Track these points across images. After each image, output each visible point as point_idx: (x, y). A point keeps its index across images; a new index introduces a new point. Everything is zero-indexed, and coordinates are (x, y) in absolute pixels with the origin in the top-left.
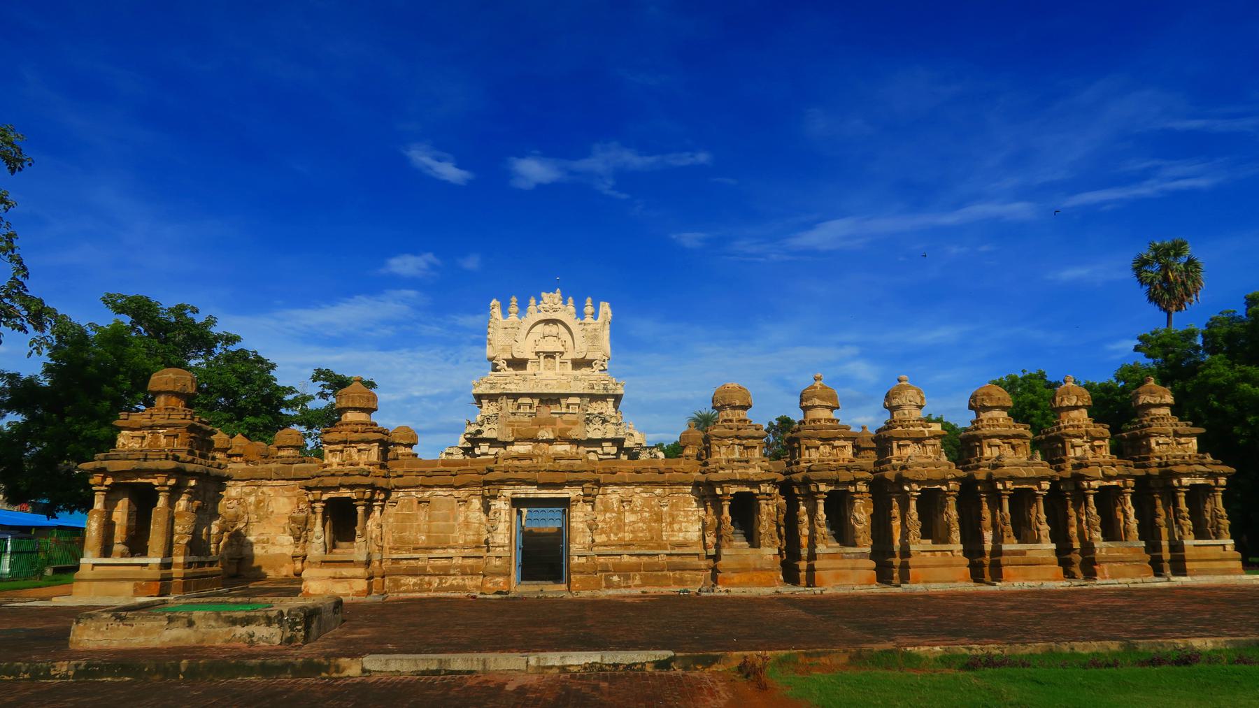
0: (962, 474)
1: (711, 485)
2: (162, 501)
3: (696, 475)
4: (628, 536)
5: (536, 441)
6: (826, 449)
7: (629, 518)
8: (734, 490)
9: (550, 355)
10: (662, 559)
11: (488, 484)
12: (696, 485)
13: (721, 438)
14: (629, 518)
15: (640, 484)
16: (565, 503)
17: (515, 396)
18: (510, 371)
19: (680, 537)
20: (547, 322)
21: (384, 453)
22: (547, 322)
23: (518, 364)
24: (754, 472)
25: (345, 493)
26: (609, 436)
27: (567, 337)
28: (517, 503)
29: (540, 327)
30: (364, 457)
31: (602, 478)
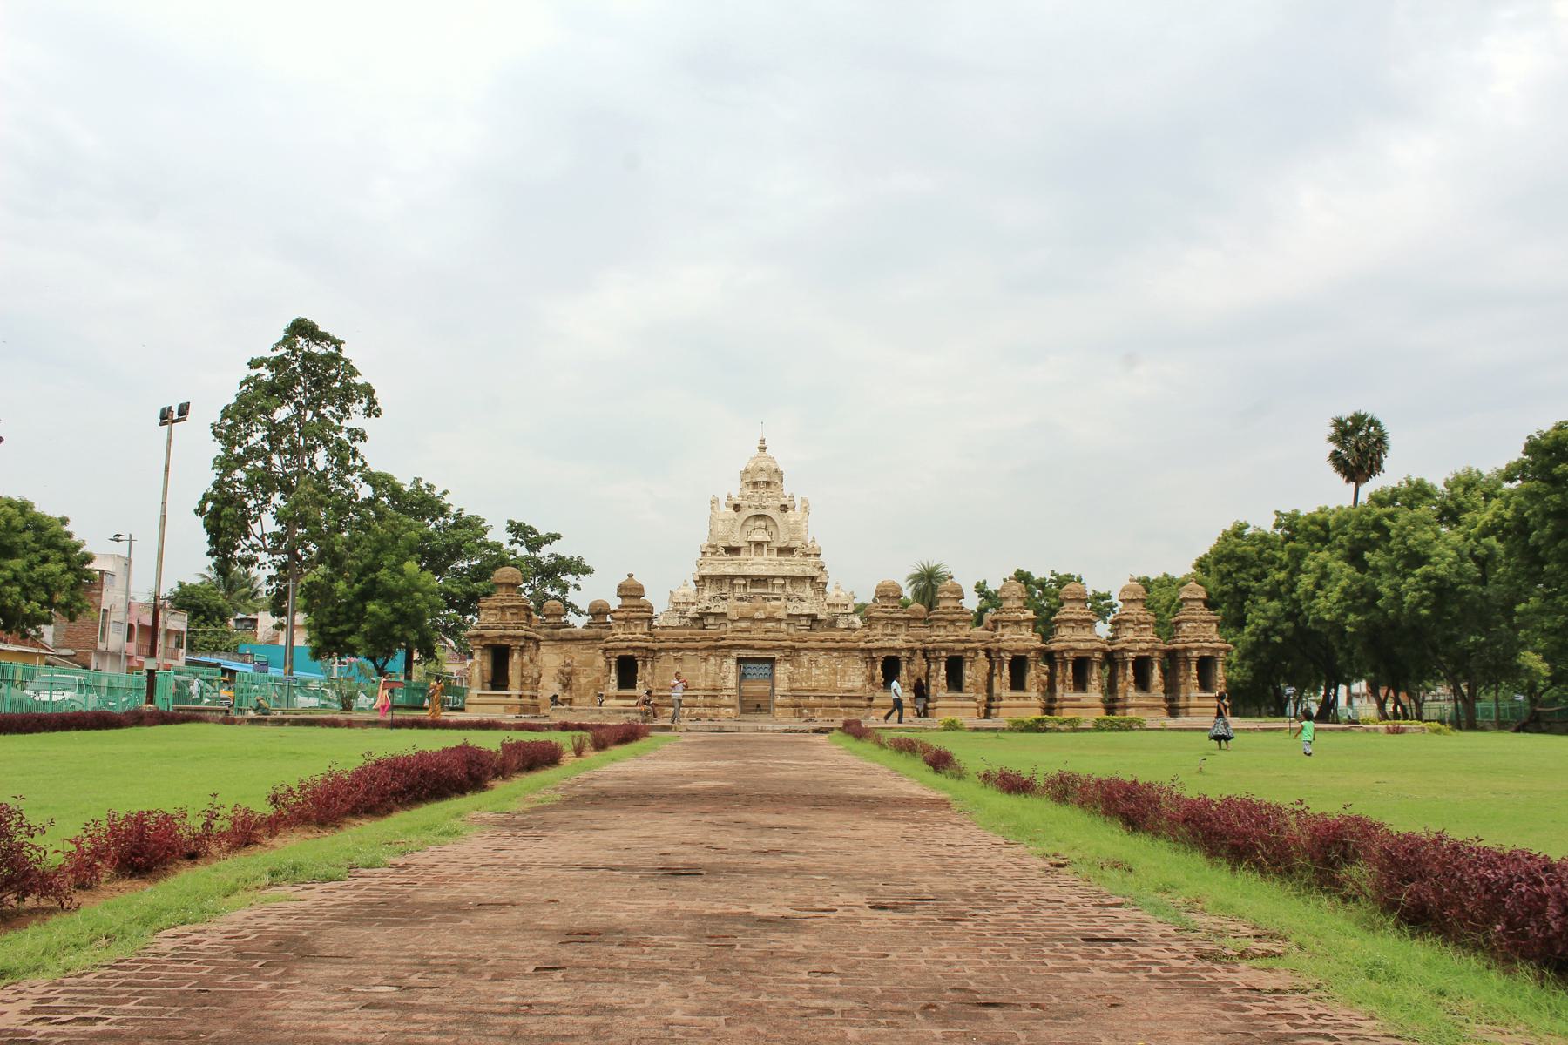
0: (1039, 645)
1: (869, 650)
2: (516, 655)
3: (862, 645)
4: (814, 684)
5: (753, 620)
6: (951, 628)
7: (815, 671)
8: (885, 654)
9: (759, 545)
10: (836, 701)
11: (718, 649)
12: (862, 650)
13: (878, 619)
14: (815, 671)
15: (823, 649)
16: (772, 661)
17: (732, 577)
18: (728, 557)
19: (849, 686)
20: (758, 517)
21: (650, 626)
22: (758, 517)
23: (733, 550)
24: (899, 642)
25: (630, 653)
26: (806, 612)
27: (771, 529)
28: (740, 660)
29: (751, 523)
30: (639, 630)
31: (797, 645)
